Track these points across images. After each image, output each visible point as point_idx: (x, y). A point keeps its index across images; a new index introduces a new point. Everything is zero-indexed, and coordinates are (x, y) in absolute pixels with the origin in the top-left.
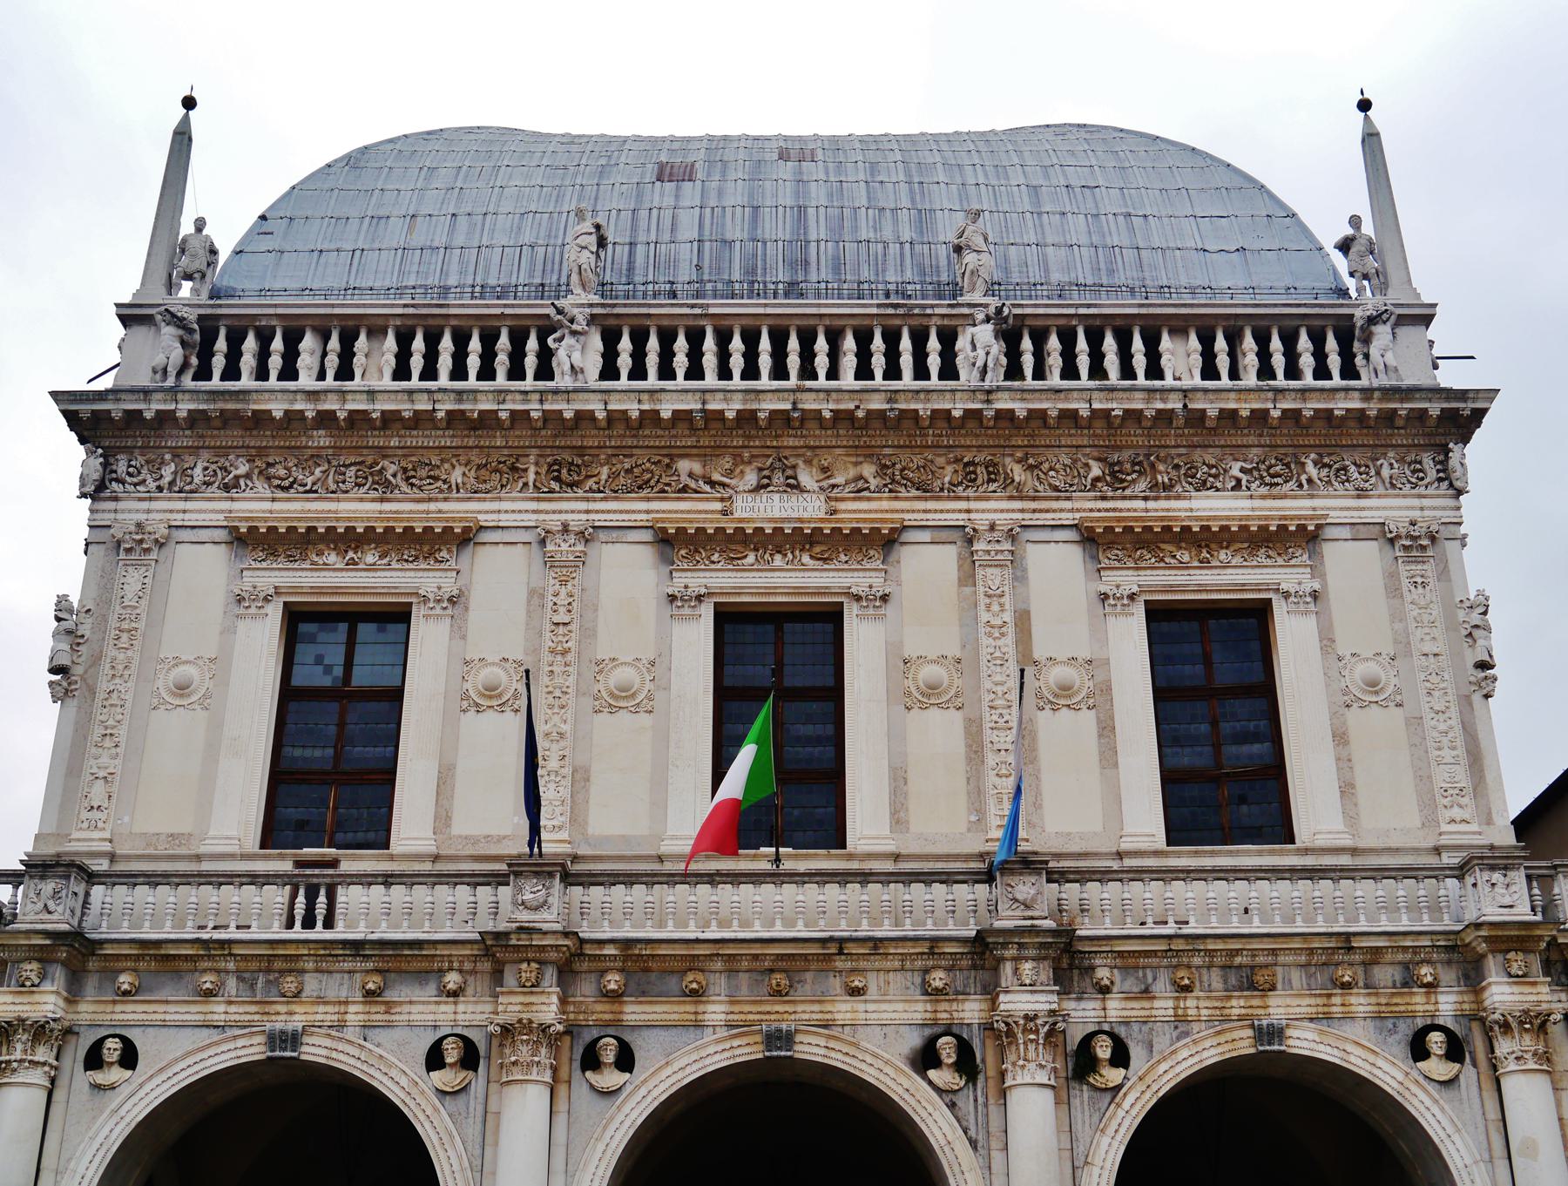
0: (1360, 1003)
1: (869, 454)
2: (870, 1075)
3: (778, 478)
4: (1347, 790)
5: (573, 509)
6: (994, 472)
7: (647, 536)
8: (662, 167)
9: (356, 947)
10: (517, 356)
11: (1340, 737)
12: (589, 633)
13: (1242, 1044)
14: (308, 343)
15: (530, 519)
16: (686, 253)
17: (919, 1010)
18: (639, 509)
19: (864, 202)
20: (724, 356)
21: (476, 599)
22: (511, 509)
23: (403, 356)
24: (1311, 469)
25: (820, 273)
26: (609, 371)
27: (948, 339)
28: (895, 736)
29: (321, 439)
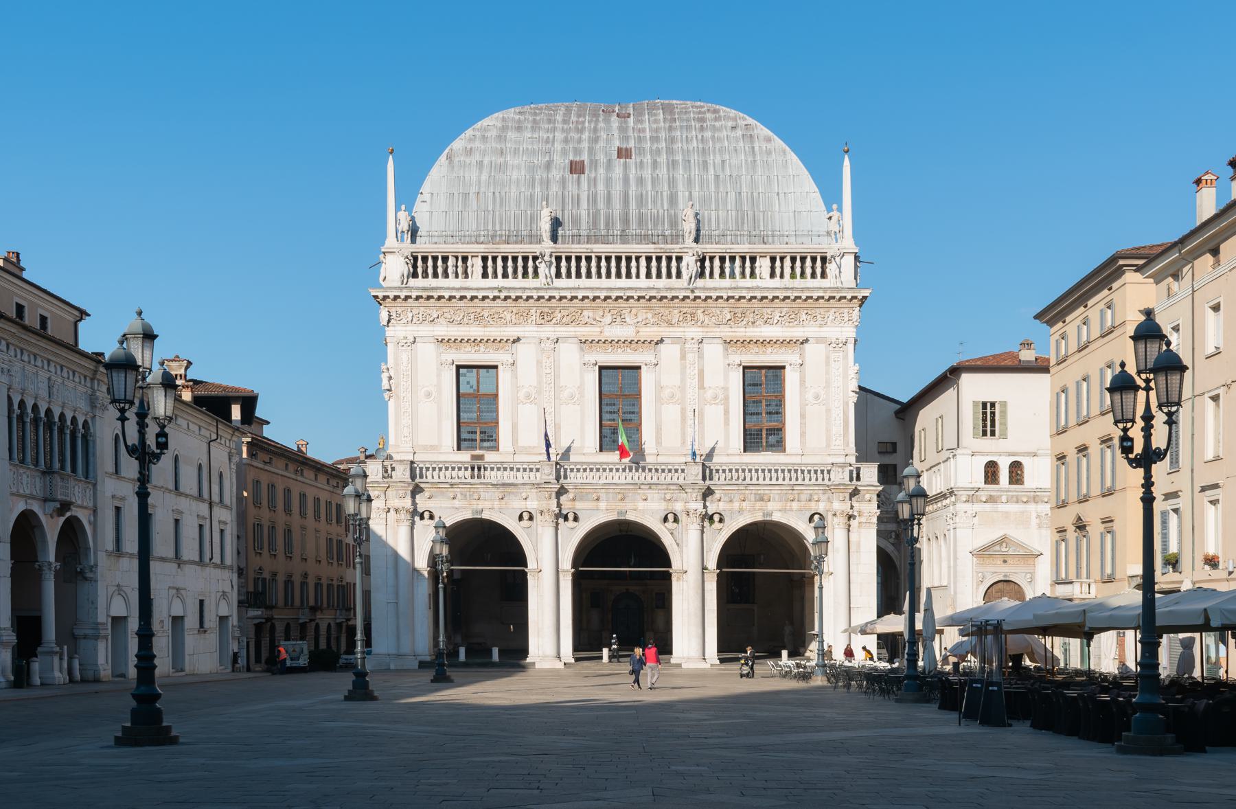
0: (795, 505)
1: (650, 308)
2: (648, 525)
3: (618, 319)
4: (803, 434)
5: (549, 331)
6: (693, 315)
7: (576, 340)
8: (571, 162)
9: (494, 485)
10: (525, 268)
11: (803, 416)
12: (557, 377)
13: (758, 517)
14: (451, 262)
15: (535, 334)
16: (584, 214)
17: (663, 505)
18: (571, 330)
19: (649, 188)
20: (599, 267)
21: (518, 363)
22: (527, 330)
23: (485, 267)
24: (804, 317)
25: (634, 229)
26: (558, 275)
27: (679, 259)
28: (658, 413)
29: (462, 304)
